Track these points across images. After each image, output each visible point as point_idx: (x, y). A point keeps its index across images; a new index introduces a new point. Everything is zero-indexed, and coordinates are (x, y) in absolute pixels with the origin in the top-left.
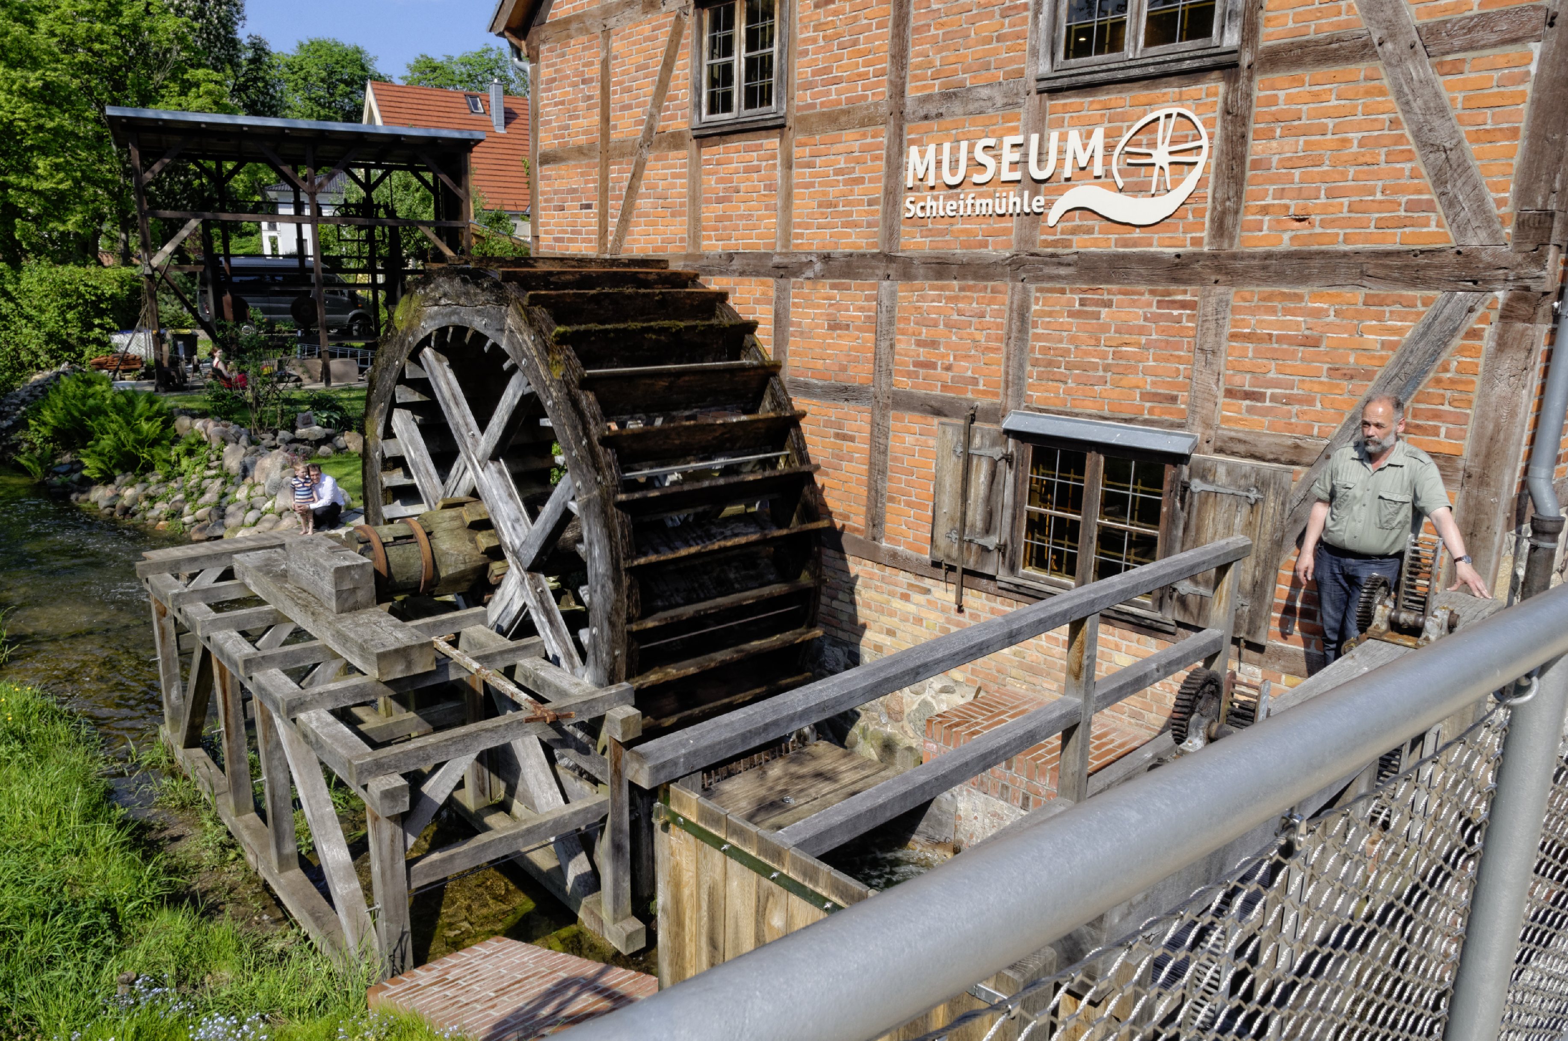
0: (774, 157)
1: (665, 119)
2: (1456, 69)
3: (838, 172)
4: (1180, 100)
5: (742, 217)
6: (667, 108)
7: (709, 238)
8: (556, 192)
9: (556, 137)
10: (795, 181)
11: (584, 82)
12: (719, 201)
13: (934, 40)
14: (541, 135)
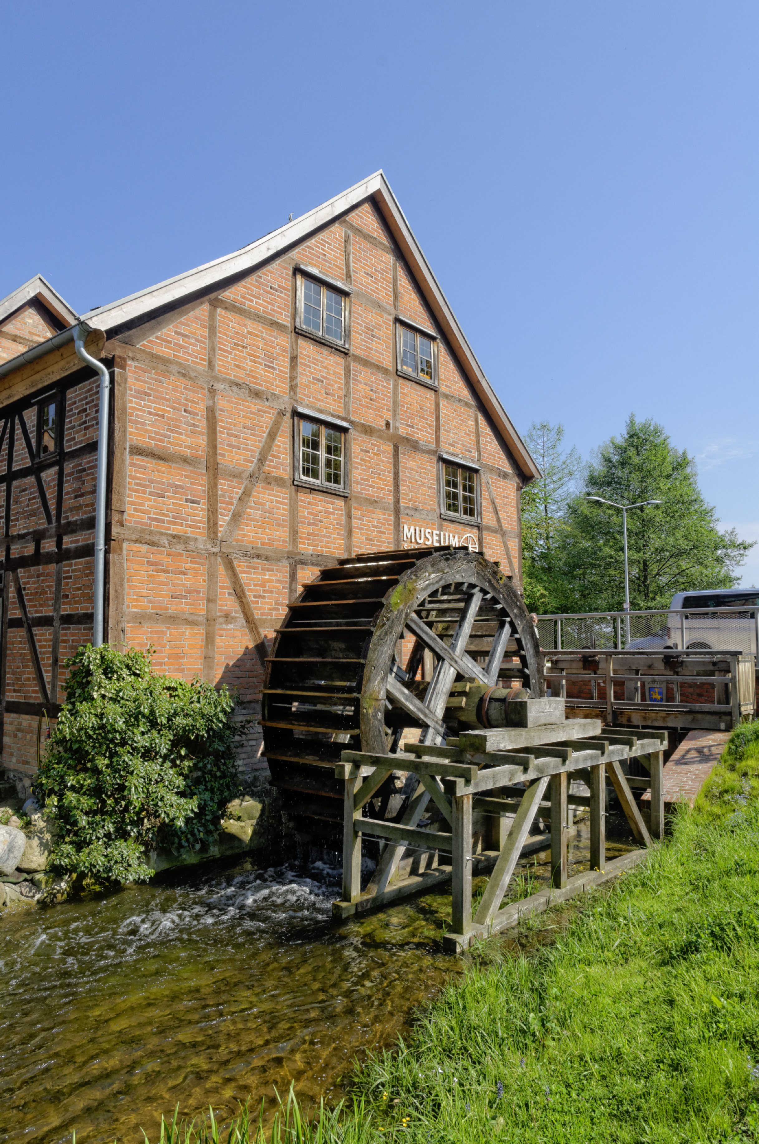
0: (342, 510)
1: (269, 466)
2: (509, 540)
3: (374, 526)
4: (470, 533)
5: (325, 536)
6: (272, 461)
7: (304, 544)
8: (151, 481)
9: (150, 438)
10: (354, 525)
11: (185, 411)
12: (310, 524)
13: (408, 486)
14: (129, 429)
